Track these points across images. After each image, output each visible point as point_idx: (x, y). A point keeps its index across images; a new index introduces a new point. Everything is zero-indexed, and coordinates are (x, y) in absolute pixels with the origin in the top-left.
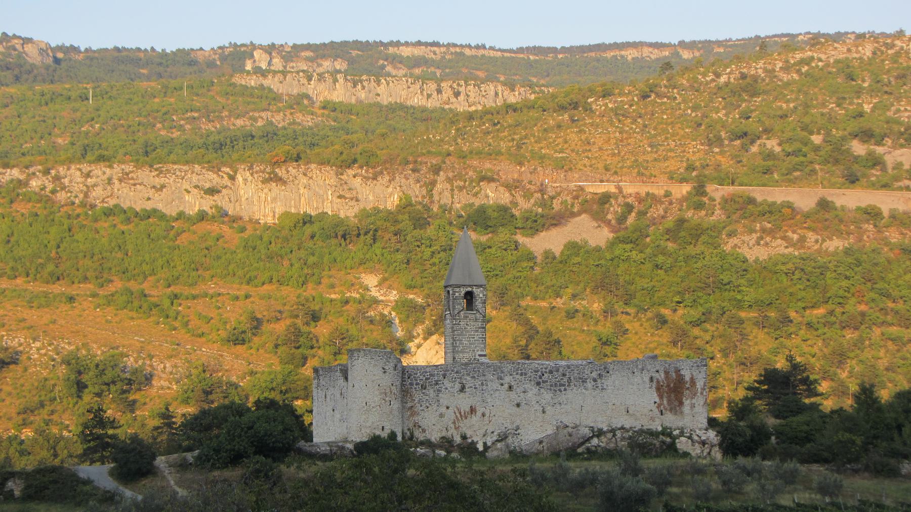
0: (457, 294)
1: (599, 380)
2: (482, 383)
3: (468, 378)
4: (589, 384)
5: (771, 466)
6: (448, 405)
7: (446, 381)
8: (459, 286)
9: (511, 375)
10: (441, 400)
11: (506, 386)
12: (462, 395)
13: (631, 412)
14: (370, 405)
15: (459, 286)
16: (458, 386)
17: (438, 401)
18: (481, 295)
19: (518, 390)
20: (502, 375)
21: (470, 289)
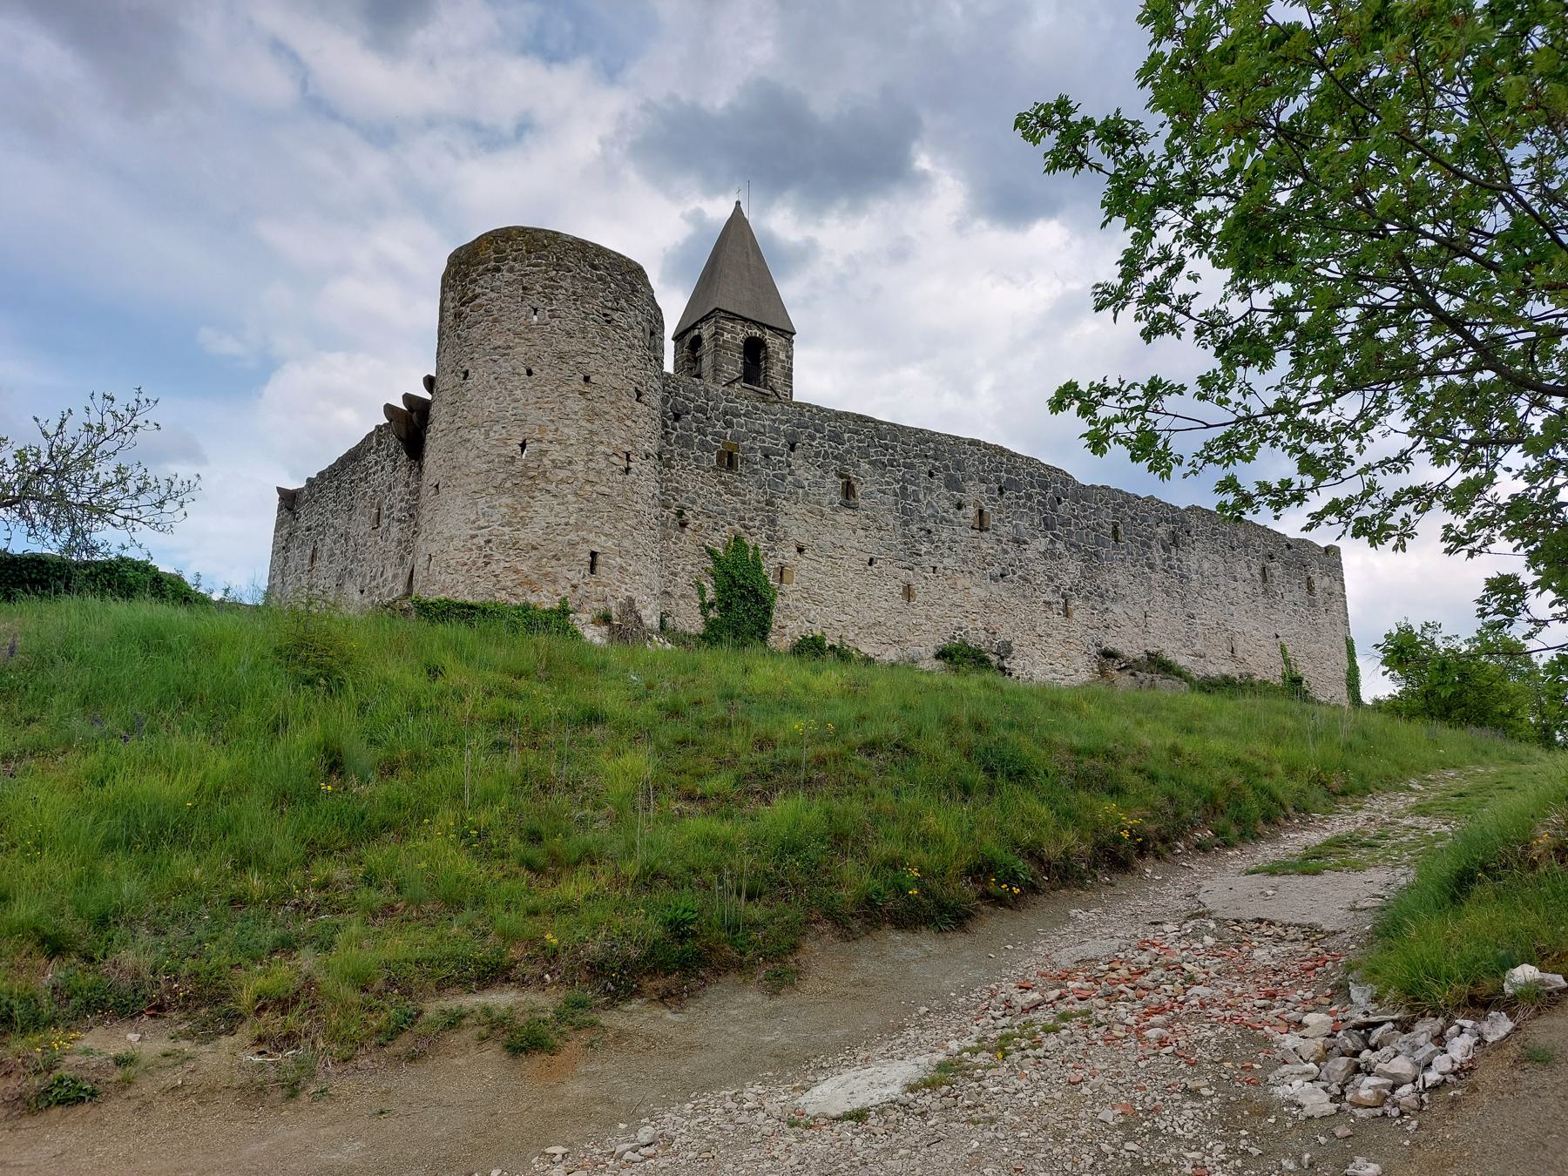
0: (727, 336)
1: (1174, 550)
2: (904, 488)
3: (865, 466)
4: (1157, 555)
5: (1440, 837)
6: (803, 541)
7: (796, 460)
8: (733, 317)
9: (982, 481)
10: (781, 520)
11: (971, 512)
12: (844, 517)
13: (1239, 654)
14: (543, 453)
15: (733, 317)
16: (832, 484)
17: (773, 522)
18: (782, 356)
19: (1002, 530)
20: (959, 475)
21: (756, 332)
